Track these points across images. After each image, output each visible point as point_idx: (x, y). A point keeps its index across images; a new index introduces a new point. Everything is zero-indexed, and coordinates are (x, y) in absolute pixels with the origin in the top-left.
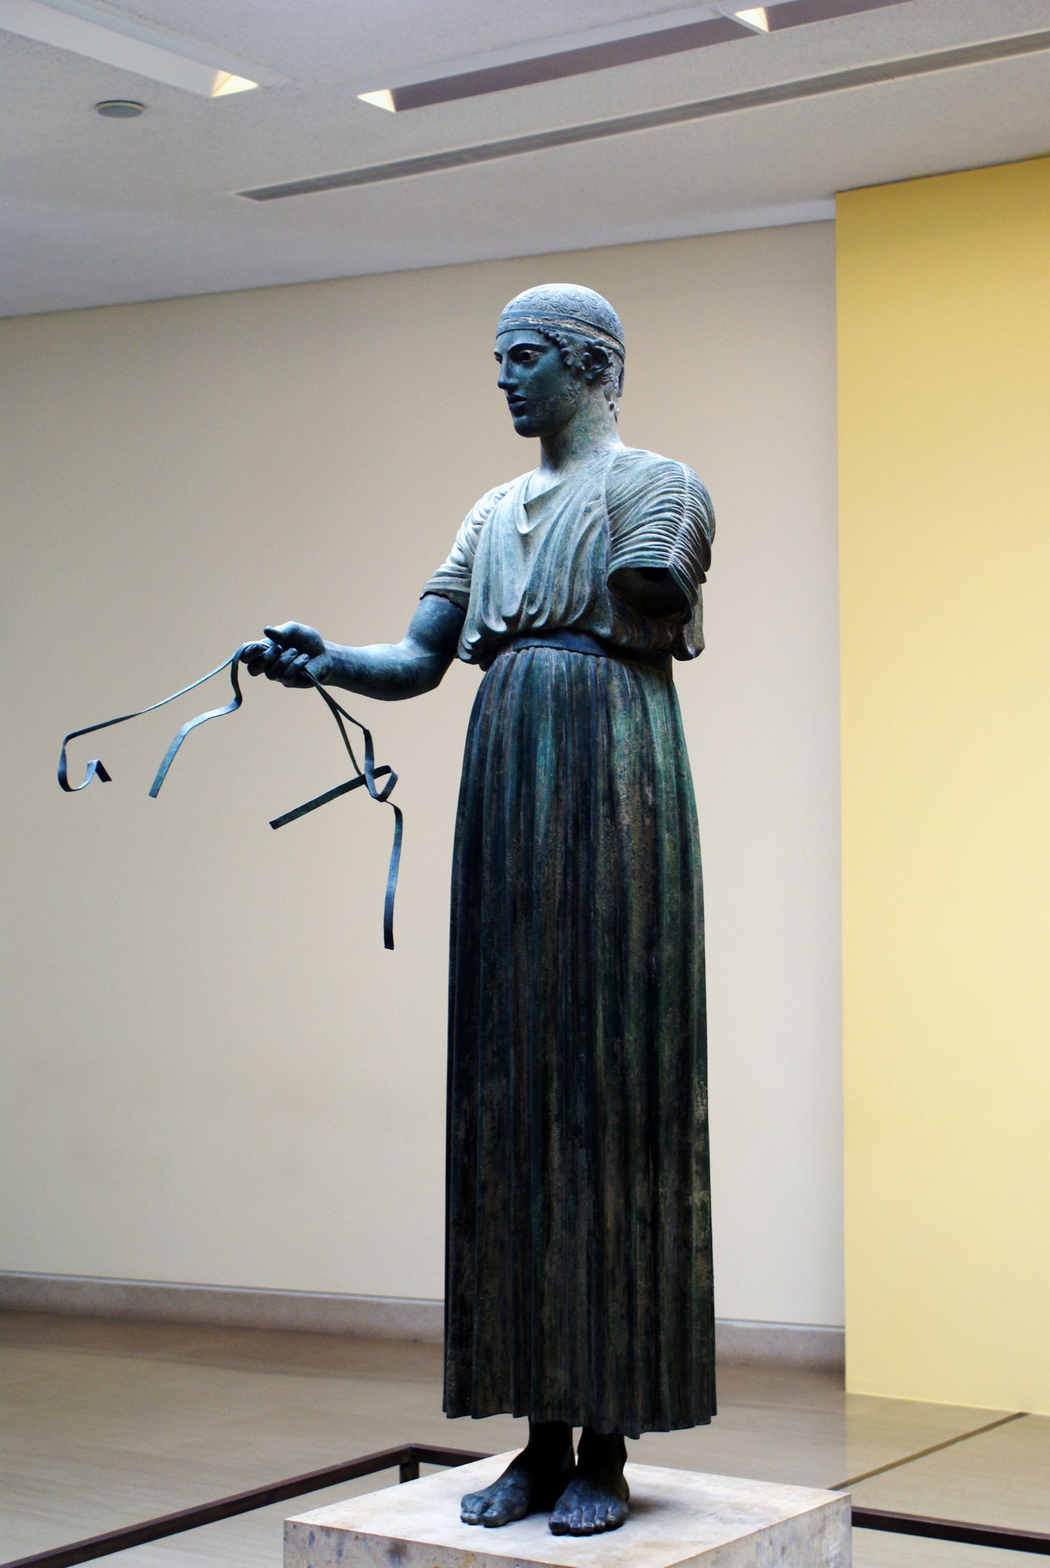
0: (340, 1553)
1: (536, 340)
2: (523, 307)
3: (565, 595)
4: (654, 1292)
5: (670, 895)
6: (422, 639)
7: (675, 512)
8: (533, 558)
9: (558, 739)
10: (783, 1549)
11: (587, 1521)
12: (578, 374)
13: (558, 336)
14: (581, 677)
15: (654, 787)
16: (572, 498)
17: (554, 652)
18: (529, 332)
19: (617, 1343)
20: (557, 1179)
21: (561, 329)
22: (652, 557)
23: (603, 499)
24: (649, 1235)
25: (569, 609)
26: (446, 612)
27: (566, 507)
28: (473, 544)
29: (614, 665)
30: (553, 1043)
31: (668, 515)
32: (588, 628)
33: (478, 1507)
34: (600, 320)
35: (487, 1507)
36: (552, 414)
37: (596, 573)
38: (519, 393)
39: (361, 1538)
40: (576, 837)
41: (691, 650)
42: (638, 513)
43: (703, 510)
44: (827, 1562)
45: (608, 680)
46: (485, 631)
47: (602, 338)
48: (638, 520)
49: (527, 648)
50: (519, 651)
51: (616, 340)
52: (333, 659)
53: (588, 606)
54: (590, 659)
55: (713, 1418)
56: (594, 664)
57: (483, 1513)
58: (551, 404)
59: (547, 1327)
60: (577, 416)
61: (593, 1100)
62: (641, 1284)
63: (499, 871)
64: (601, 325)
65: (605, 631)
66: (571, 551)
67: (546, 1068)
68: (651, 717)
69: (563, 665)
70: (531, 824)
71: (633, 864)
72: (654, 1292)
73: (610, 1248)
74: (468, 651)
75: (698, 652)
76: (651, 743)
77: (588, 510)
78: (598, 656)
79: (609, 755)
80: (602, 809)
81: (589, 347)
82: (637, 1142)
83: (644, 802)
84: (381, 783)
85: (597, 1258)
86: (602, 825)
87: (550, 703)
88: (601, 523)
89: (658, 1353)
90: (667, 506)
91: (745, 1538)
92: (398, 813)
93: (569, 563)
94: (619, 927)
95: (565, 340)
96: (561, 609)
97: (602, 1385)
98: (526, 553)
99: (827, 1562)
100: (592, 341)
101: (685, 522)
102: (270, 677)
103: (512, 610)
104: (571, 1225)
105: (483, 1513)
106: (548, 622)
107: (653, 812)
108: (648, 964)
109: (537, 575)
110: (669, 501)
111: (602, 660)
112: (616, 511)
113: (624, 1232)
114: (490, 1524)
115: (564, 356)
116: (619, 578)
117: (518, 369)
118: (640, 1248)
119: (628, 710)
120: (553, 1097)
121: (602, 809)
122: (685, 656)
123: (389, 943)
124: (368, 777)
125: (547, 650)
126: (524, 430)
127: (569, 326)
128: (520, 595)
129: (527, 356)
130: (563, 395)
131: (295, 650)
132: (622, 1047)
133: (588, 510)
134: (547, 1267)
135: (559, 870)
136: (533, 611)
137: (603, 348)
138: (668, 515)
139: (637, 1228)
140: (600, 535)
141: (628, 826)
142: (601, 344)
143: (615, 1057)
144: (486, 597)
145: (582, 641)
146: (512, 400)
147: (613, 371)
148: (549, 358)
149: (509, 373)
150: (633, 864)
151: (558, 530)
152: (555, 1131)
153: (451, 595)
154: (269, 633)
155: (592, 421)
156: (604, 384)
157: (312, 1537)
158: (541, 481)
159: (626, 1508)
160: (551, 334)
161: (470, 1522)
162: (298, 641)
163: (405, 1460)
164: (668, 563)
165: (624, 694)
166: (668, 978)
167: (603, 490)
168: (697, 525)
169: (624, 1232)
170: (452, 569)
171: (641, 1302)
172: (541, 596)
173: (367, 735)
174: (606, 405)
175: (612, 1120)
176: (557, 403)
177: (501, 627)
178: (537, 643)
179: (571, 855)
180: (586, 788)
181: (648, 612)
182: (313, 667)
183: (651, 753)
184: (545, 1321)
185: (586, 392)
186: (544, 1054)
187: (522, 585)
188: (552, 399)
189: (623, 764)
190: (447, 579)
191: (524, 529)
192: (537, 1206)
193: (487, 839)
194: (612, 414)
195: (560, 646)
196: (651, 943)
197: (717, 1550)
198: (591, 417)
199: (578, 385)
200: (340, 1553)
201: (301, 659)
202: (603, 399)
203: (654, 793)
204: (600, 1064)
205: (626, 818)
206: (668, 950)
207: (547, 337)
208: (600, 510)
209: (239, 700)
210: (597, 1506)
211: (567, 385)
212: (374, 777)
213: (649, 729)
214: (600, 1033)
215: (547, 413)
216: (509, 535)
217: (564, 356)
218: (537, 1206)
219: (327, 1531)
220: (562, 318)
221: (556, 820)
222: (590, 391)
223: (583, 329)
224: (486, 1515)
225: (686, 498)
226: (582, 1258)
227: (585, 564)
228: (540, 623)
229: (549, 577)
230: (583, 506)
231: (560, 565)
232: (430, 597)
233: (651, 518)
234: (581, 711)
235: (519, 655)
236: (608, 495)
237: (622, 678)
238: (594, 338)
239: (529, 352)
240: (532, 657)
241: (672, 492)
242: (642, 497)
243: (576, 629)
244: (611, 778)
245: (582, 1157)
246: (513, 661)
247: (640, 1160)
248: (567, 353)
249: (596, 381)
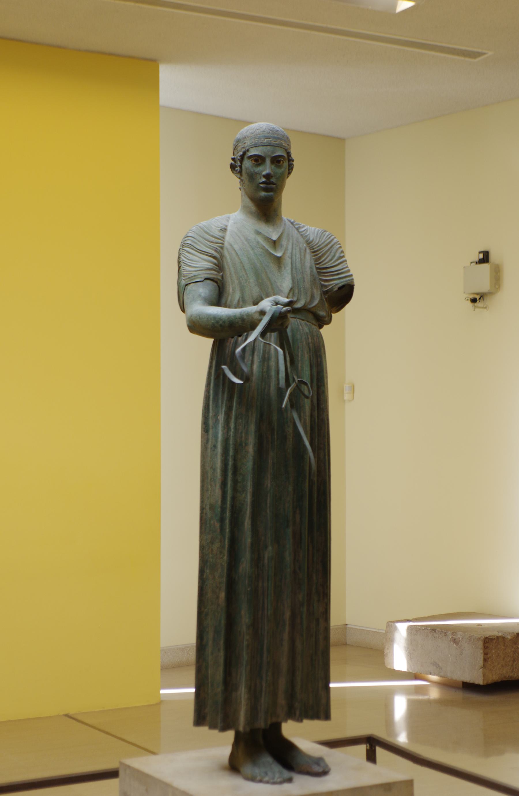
16: (293, 241)
17: (302, 322)
18: (283, 150)
27: (293, 245)
38: (273, 180)
42: (334, 256)
48: (338, 259)
65: (322, 313)
77: (306, 250)
78: (315, 325)
117: (273, 166)
125: (298, 320)
129: (279, 162)
136: (295, 299)
145: (310, 316)
153: (219, 282)
161: (281, 783)
191: (279, 254)
195: (304, 318)
216: (261, 255)
229: (298, 282)
232: (209, 282)
242: (331, 247)
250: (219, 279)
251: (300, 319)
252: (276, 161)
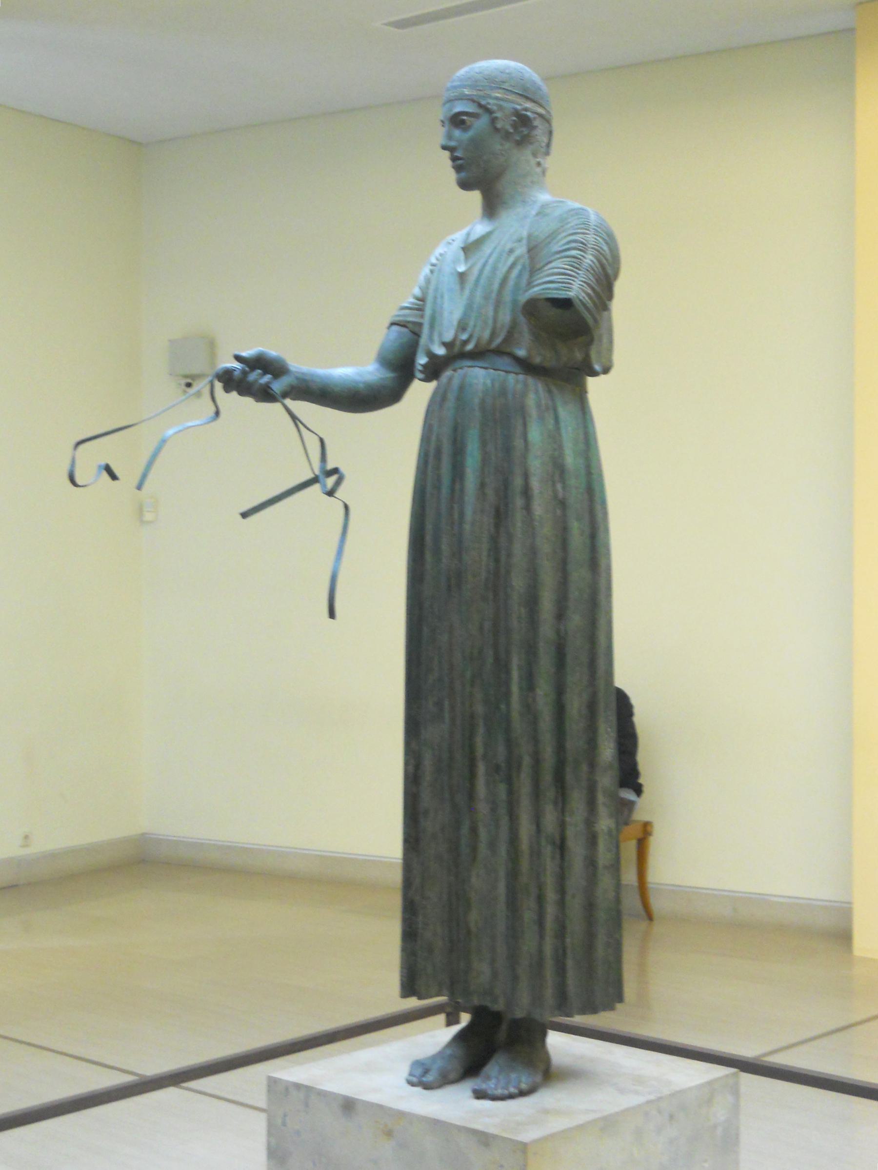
0: (307, 1105)
1: (470, 108)
2: (461, 80)
3: (490, 322)
4: (562, 903)
5: (579, 575)
6: (385, 361)
8: (467, 292)
9: (484, 443)
10: (671, 1117)
11: (503, 1088)
12: (507, 136)
13: (489, 103)
14: (503, 392)
15: (564, 483)
18: (465, 102)
19: (528, 944)
20: (483, 808)
23: (524, 242)
24: (558, 856)
25: (493, 334)
26: (405, 340)
28: (428, 281)
29: (531, 380)
30: (479, 696)
31: (574, 253)
32: (508, 350)
33: (418, 1072)
34: (526, 89)
35: (426, 1072)
37: (515, 302)
38: (458, 154)
39: (323, 1095)
40: (497, 525)
41: (597, 367)
43: (605, 248)
44: (715, 1127)
45: (524, 394)
46: (431, 355)
47: (528, 105)
49: (461, 368)
50: (455, 370)
51: (541, 106)
52: (297, 378)
53: (509, 332)
54: (511, 378)
55: (619, 1006)
56: (515, 380)
57: (427, 1077)
59: (474, 929)
61: (510, 743)
62: (551, 896)
63: (437, 551)
64: (528, 93)
65: (521, 353)
66: (496, 286)
67: (472, 716)
68: (562, 425)
69: (489, 382)
70: (462, 514)
71: (545, 548)
72: (562, 903)
73: (525, 864)
74: (420, 371)
75: (606, 370)
76: (560, 447)
78: (516, 374)
79: (524, 457)
80: (519, 502)
81: (517, 113)
82: (547, 777)
83: (555, 496)
84: (331, 481)
85: (513, 874)
86: (519, 516)
87: (478, 414)
88: (522, 261)
89: (564, 951)
90: (574, 245)
91: (633, 1108)
92: (346, 507)
93: (494, 296)
94: (532, 601)
95: (495, 108)
96: (487, 334)
97: (515, 978)
98: (462, 288)
99: (715, 1127)
100: (518, 107)
101: (589, 259)
102: (241, 393)
103: (448, 337)
104: (492, 845)
105: (427, 1077)
106: (476, 346)
107: (563, 504)
108: (558, 632)
109: (469, 307)
110: (575, 241)
111: (521, 377)
112: (533, 250)
113: (535, 853)
114: (427, 1087)
115: (494, 120)
116: (532, 308)
117: (457, 133)
118: (550, 866)
119: (541, 418)
120: (479, 741)
121: (519, 502)
122: (594, 374)
123: (332, 614)
124: (321, 477)
125: (477, 370)
126: (465, 185)
128: (455, 323)
129: (463, 122)
131: (259, 371)
132: (534, 700)
133: (511, 251)
134: (474, 880)
135: (485, 553)
136: (464, 337)
137: (529, 114)
138: (574, 253)
139: (547, 850)
140: (521, 271)
141: (540, 516)
142: (526, 110)
143: (529, 710)
144: (432, 327)
145: (504, 362)
146: (454, 159)
147: (539, 133)
148: (481, 124)
149: (449, 137)
150: (545, 548)
151: (488, 268)
152: (481, 769)
153: (410, 325)
154: (238, 358)
157: (287, 1089)
158: (480, 228)
159: (546, 1073)
160: (483, 102)
161: (412, 1084)
162: (261, 363)
163: (449, 1010)
164: (571, 294)
165: (539, 406)
166: (576, 644)
167: (525, 234)
169: (535, 853)
170: (413, 304)
171: (551, 910)
172: (471, 323)
173: (322, 441)
174: (533, 161)
175: (527, 761)
177: (441, 351)
178: (469, 363)
179: (494, 540)
180: (506, 485)
181: (559, 337)
182: (277, 387)
183: (561, 455)
184: (472, 926)
186: (471, 706)
187: (457, 315)
188: (485, 158)
189: (537, 465)
190: (407, 312)
191: (461, 268)
192: (465, 830)
193: (429, 527)
194: (538, 170)
196: (560, 615)
197: (605, 1119)
199: (507, 145)
200: (307, 1105)
201: (267, 378)
202: (530, 157)
203: (564, 488)
204: (515, 715)
205: (539, 509)
206: (576, 620)
207: (480, 106)
208: (521, 250)
209: (217, 413)
210: (513, 1076)
211: (497, 145)
212: (328, 478)
213: (560, 435)
214: (515, 689)
217: (494, 120)
218: (465, 830)
219: (298, 1086)
220: (492, 88)
221: (482, 511)
223: (511, 97)
224: (424, 1079)
225: (591, 238)
226: (502, 873)
227: (507, 297)
228: (470, 347)
230: (509, 246)
231: (486, 298)
232: (395, 328)
233: (558, 256)
234: (502, 420)
235: (456, 375)
236: (530, 236)
237: (537, 392)
238: (521, 105)
239: (465, 118)
240: (465, 376)
243: (499, 352)
244: (526, 476)
245: (502, 788)
246: (450, 379)
247: (550, 793)
248: (496, 118)
249: (523, 141)
250: (409, 322)
251: (481, 367)
252: (457, 121)
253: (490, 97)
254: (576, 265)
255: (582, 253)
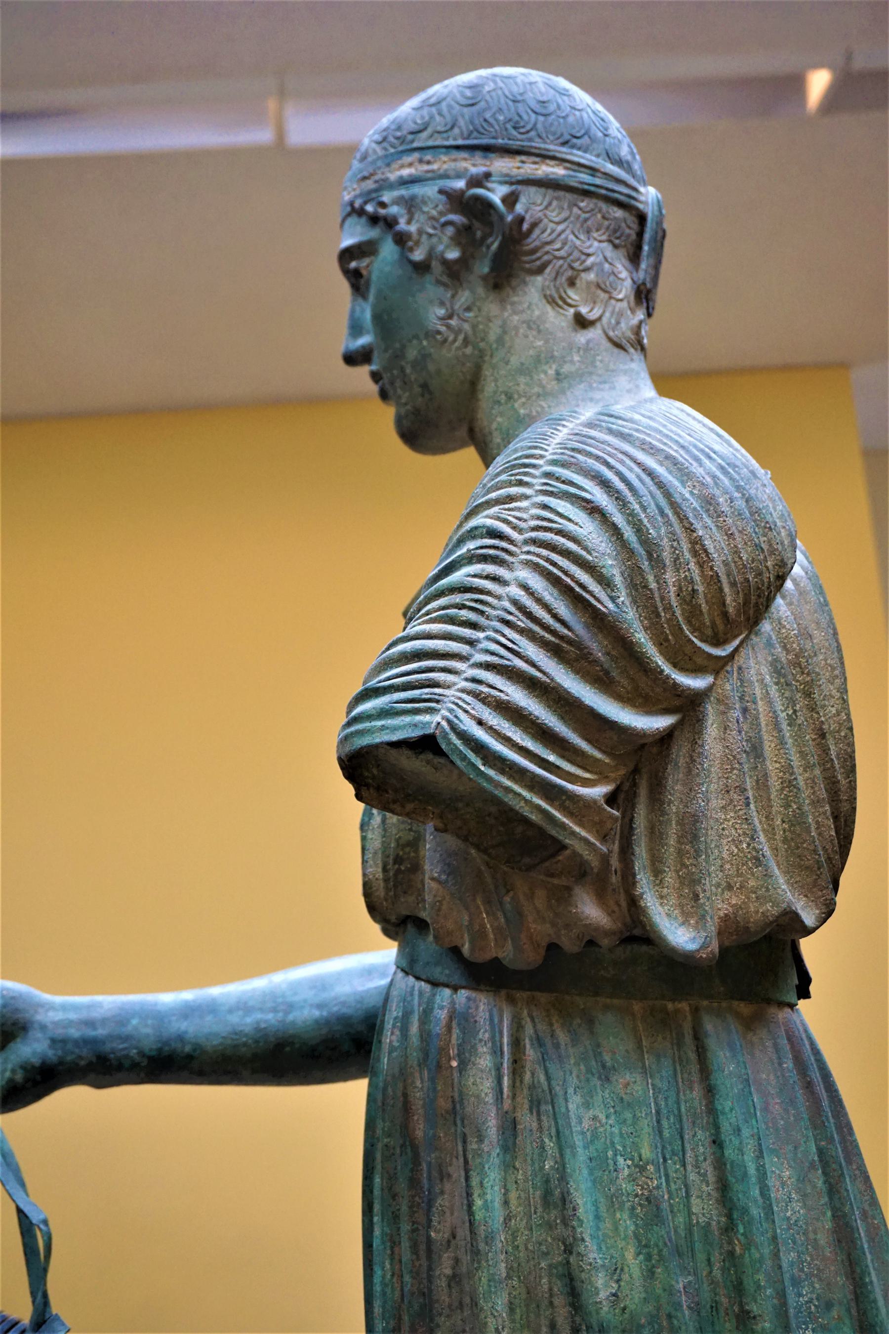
7: (484, 559)
12: (455, 273)
21: (391, 186)
22: (384, 713)
36: (425, 386)
43: (586, 527)
51: (545, 157)
58: (415, 364)
60: (487, 372)
81: (458, 201)
100: (461, 184)
127: (406, 172)
130: (431, 334)
155: (523, 370)
156: (540, 270)
168: (555, 581)
174: (557, 321)
176: (425, 357)
185: (492, 308)
188: (412, 353)
194: (594, 334)
198: (514, 361)
199: (464, 297)
215: (417, 390)
220: (389, 161)
222: (503, 302)
241: (489, 504)
253: (385, 185)
254: (465, 614)
255: (490, 569)
